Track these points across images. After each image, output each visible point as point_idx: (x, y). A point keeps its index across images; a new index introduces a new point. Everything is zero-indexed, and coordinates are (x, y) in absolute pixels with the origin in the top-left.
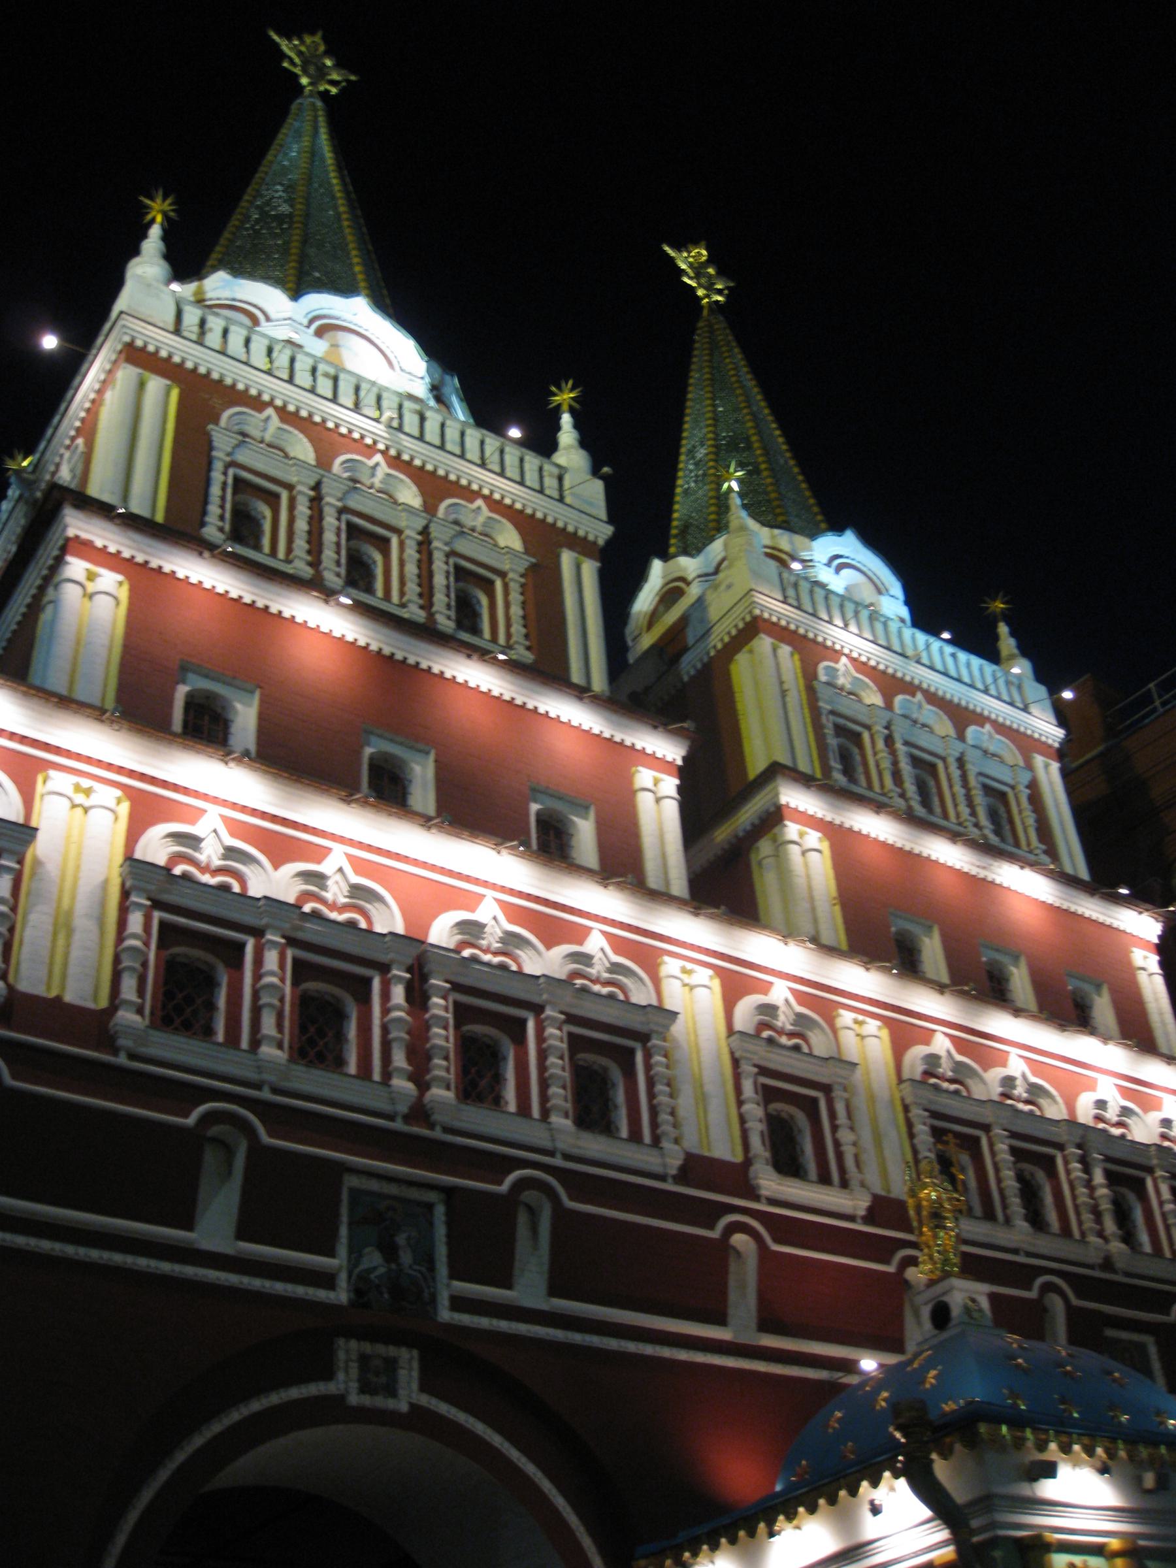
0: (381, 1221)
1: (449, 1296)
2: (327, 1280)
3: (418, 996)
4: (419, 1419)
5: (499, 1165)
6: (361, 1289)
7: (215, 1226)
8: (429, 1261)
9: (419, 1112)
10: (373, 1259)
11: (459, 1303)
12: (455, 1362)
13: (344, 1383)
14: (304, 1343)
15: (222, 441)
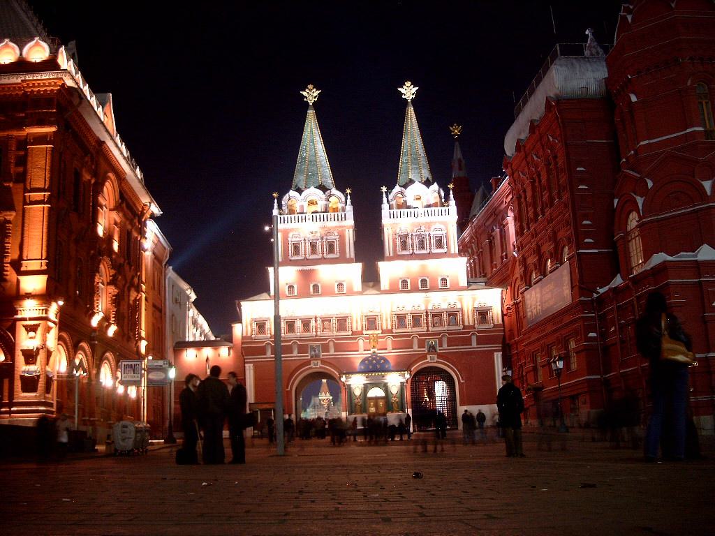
0: (313, 349)
1: (322, 355)
2: (308, 356)
3: (316, 321)
4: (321, 367)
5: (326, 339)
6: (312, 357)
7: (295, 353)
8: (319, 351)
9: (316, 336)
10: (313, 353)
11: (323, 355)
12: (323, 362)
13: (312, 365)
14: (308, 362)
15: (289, 239)
